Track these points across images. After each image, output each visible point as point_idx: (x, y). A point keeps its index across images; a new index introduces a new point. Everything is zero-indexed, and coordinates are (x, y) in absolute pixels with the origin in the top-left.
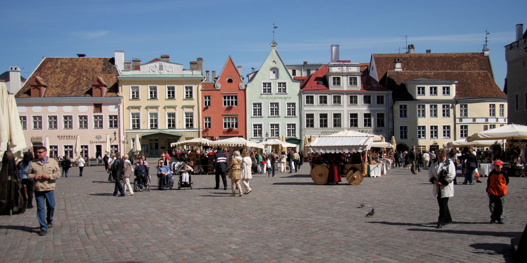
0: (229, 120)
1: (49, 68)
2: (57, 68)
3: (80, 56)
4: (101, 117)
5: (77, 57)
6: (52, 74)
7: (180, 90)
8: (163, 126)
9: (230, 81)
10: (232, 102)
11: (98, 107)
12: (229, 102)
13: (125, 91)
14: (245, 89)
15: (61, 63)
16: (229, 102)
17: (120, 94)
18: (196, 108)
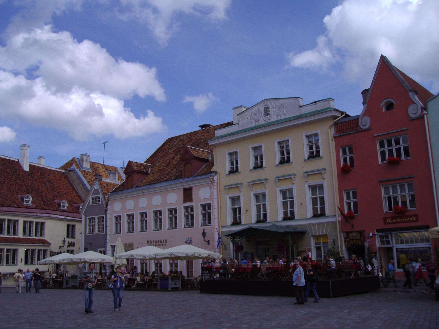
0: (395, 191)
1: (165, 150)
2: (172, 148)
3: (202, 126)
4: (192, 208)
5: (200, 128)
6: (162, 157)
7: (299, 148)
8: (275, 215)
9: (390, 106)
10: (398, 150)
11: (188, 194)
12: (391, 151)
13: (221, 163)
14: (422, 118)
15: (180, 141)
16: (391, 151)
17: (214, 169)
18: (327, 175)
